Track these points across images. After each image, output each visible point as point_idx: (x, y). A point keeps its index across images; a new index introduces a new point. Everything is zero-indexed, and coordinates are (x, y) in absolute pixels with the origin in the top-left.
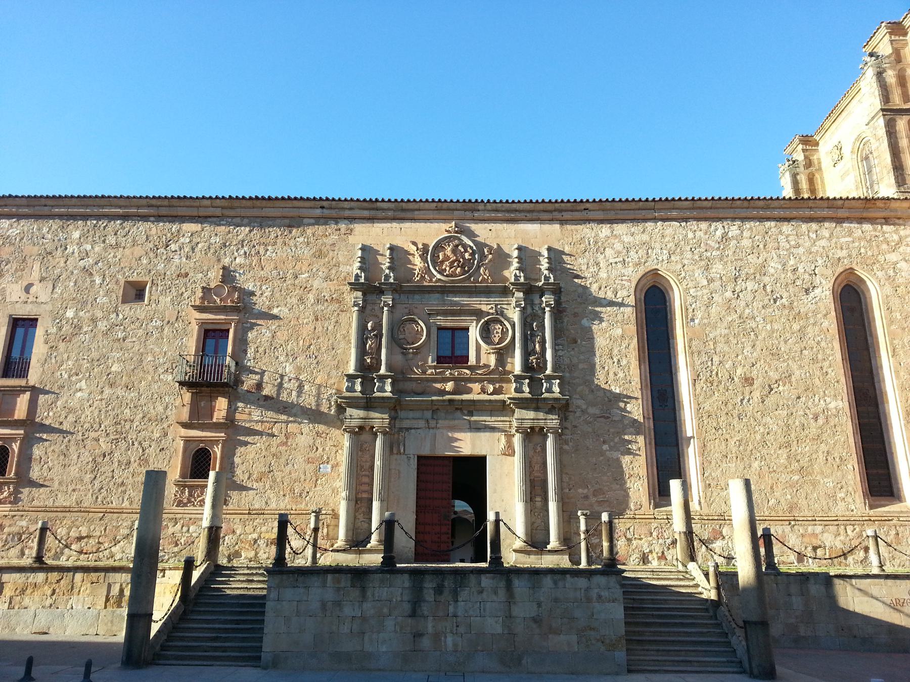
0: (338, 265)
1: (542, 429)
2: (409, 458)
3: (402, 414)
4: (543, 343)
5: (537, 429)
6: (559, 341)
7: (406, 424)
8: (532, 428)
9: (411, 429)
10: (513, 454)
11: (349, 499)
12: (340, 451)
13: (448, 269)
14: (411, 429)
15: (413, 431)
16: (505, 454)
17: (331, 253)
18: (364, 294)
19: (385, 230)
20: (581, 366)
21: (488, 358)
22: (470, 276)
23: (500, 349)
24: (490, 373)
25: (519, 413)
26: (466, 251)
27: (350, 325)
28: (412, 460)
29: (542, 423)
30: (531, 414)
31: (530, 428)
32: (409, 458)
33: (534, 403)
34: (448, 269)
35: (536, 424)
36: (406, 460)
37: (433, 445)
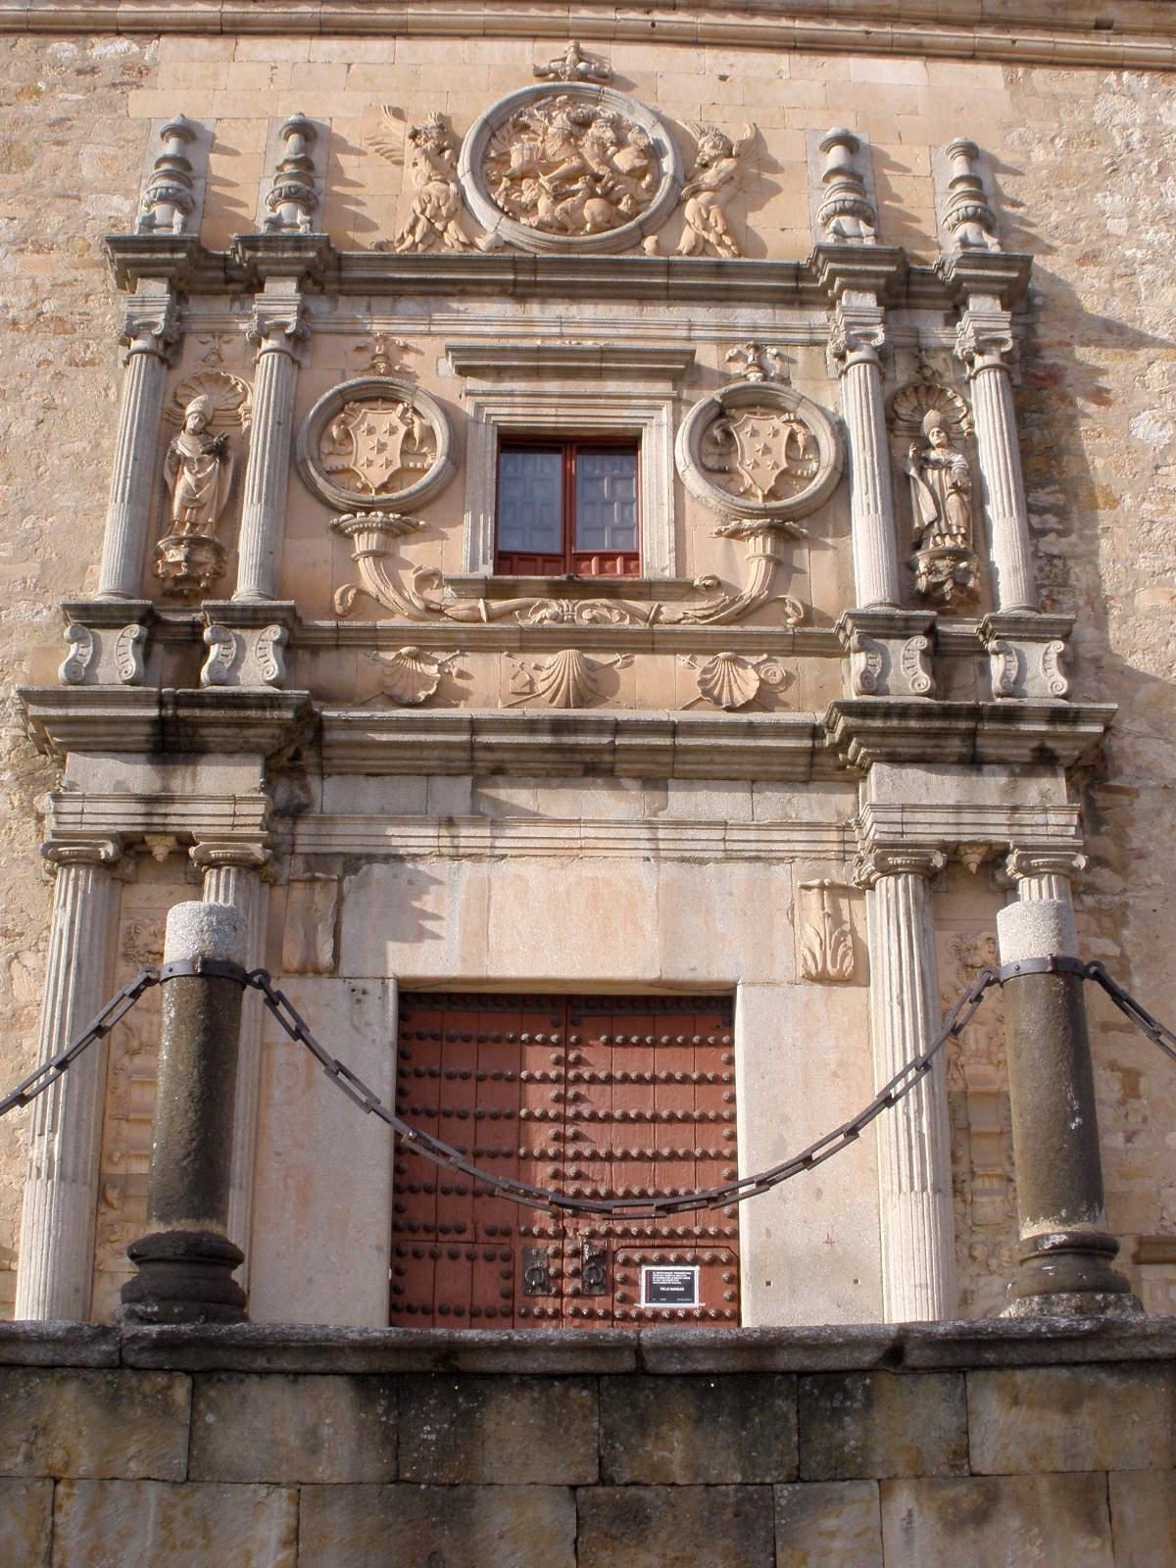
0: (71, 195)
1: (995, 856)
2: (358, 996)
3: (328, 794)
4: (973, 492)
5: (973, 860)
6: (1043, 497)
7: (346, 838)
8: (953, 851)
9: (371, 858)
10: (858, 976)
11: (65, 1175)
12: (30, 959)
13: (543, 203)
14: (371, 858)
15: (379, 870)
16: (821, 978)
17: (52, 153)
18: (180, 294)
19: (284, 71)
20: (1144, 600)
21: (730, 561)
22: (642, 231)
23: (787, 514)
24: (745, 614)
25: (880, 781)
26: (620, 143)
27: (108, 418)
28: (372, 1003)
29: (996, 829)
30: (944, 787)
31: (943, 847)
32: (358, 996)
33: (953, 731)
34: (543, 203)
35: (967, 832)
36: (344, 1004)
37: (478, 937)
